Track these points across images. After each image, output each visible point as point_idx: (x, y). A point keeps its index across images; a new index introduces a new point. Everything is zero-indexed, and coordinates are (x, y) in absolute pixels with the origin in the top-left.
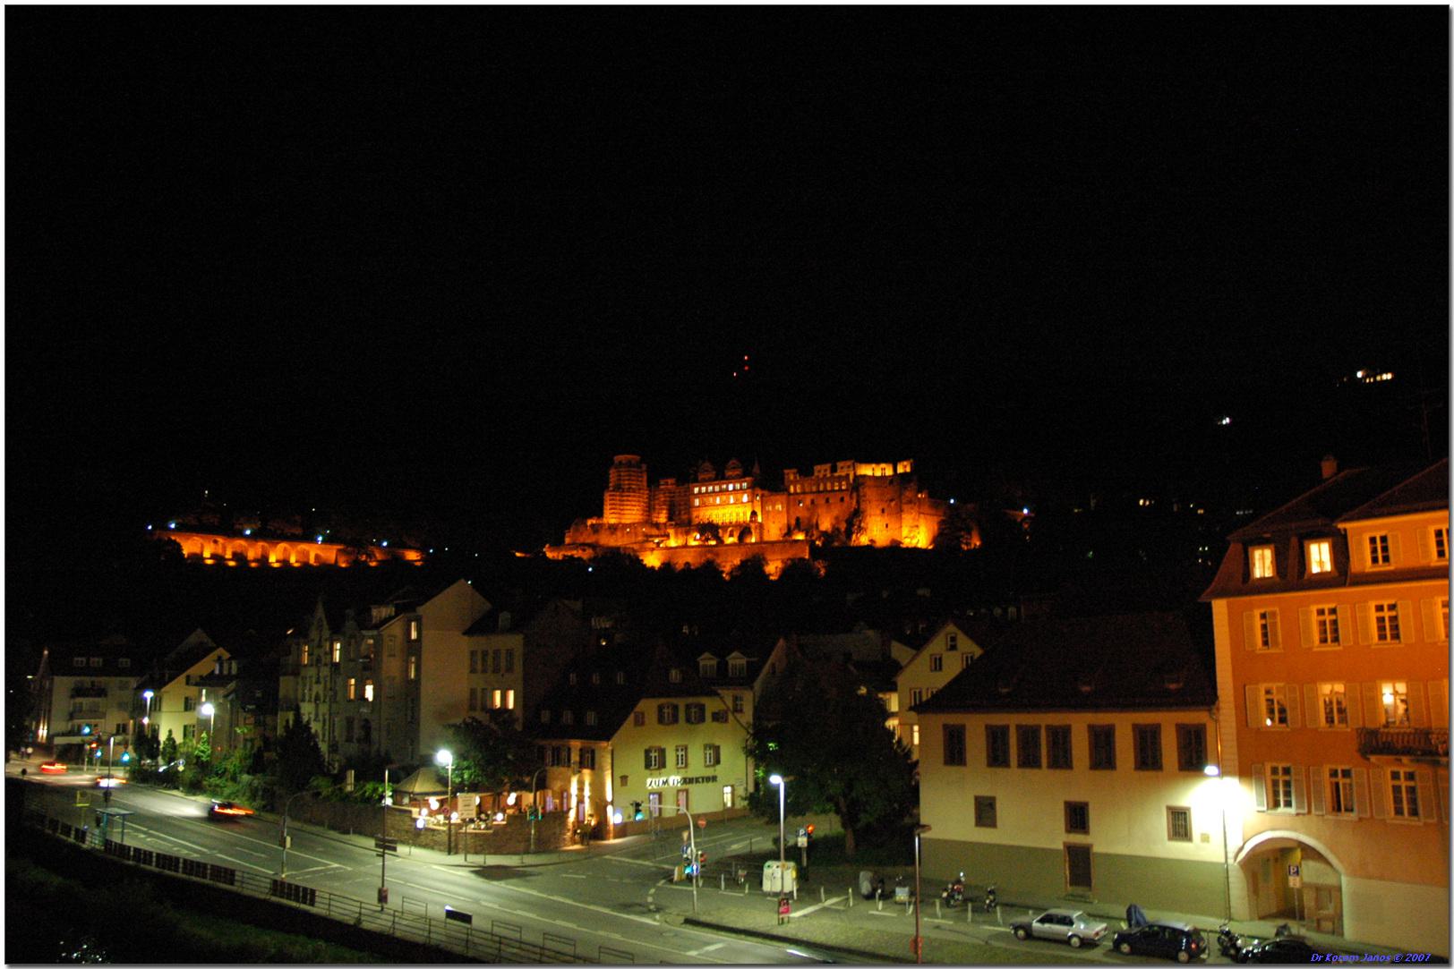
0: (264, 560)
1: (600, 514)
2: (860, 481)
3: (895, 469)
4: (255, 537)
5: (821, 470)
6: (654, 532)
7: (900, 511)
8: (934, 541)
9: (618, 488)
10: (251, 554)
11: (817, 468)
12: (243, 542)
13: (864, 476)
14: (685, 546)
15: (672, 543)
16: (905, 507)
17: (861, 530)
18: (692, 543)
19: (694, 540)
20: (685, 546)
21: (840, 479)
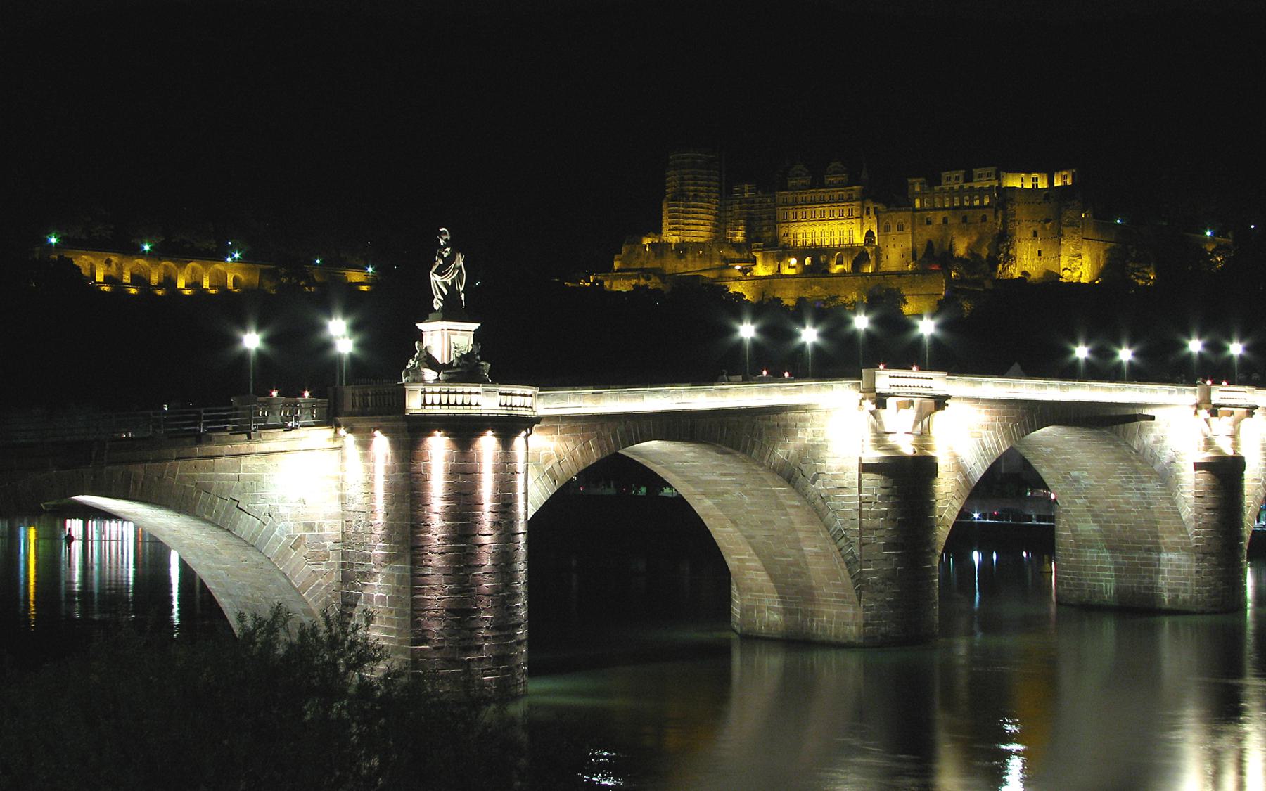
0: (169, 282)
1: (658, 231)
2: (1007, 195)
3: (1051, 182)
4: (155, 255)
5: (952, 180)
6: (735, 255)
7: (1059, 235)
8: (1102, 273)
9: (680, 195)
10: (154, 279)
11: (945, 174)
12: (142, 262)
13: (1014, 188)
14: (778, 275)
15: (761, 270)
16: (1065, 230)
17: (1010, 259)
18: (786, 271)
19: (790, 267)
20: (778, 275)
21: (982, 192)
